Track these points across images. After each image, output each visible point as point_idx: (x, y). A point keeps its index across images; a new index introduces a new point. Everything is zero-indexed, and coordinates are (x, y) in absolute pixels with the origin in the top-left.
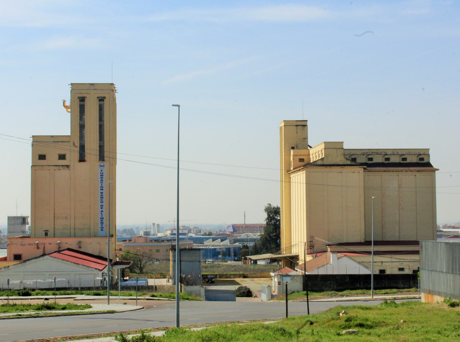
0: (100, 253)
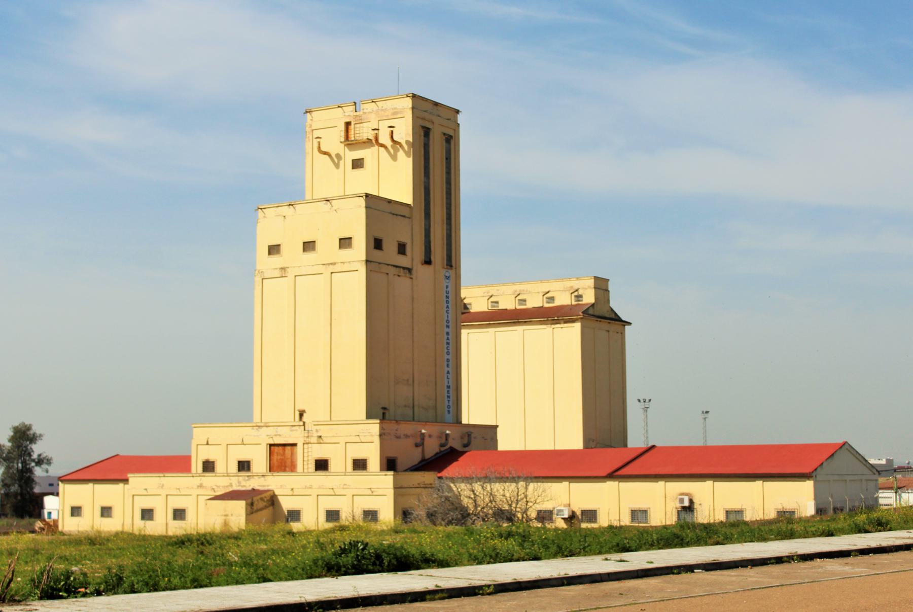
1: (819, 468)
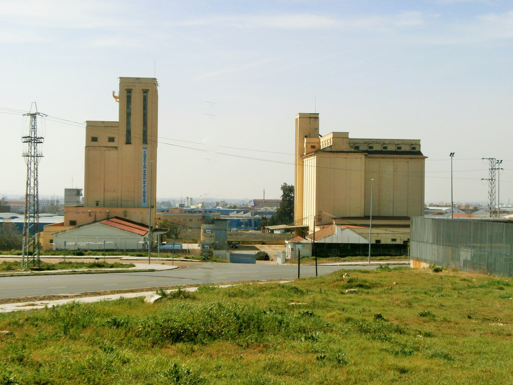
0: (142, 221)
1: (60, 233)
